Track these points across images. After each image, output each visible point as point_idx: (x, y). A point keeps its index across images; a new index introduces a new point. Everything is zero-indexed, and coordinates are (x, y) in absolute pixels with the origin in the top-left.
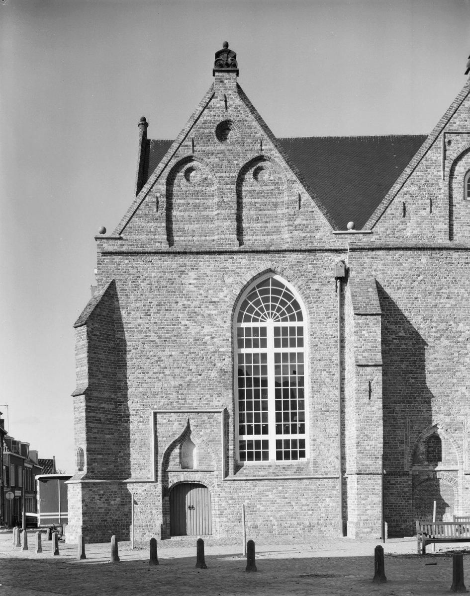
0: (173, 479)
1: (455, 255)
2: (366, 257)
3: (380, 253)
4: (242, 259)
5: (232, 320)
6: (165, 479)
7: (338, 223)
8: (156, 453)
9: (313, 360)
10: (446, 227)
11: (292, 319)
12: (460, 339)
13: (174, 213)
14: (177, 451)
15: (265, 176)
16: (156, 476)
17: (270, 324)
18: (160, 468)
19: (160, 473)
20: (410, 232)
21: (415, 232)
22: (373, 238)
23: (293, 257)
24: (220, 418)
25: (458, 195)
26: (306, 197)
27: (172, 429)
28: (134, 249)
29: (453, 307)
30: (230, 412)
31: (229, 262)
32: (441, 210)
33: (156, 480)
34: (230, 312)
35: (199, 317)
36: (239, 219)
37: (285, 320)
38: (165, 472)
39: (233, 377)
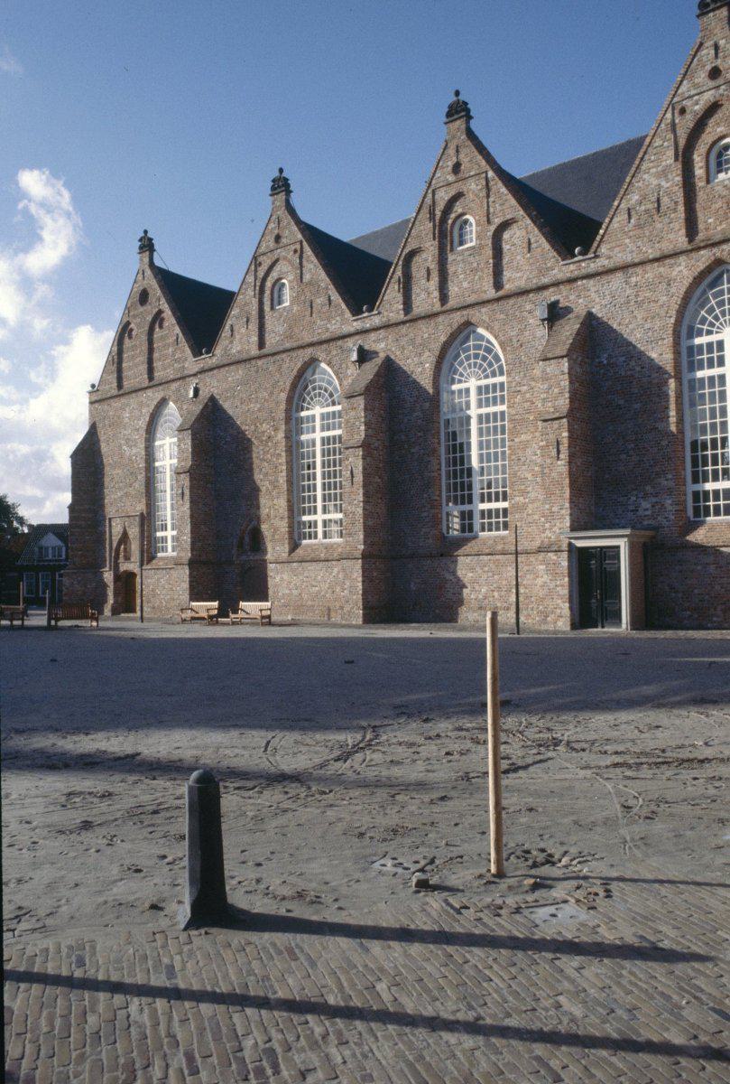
1: (260, 363)
2: (207, 377)
3: (215, 371)
4: (149, 393)
7: (197, 352)
10: (256, 339)
13: (124, 365)
15: (166, 324)
20: (236, 348)
21: (238, 349)
22: (214, 360)
23: (174, 386)
25: (267, 308)
26: (181, 335)
27: (117, 530)
28: (104, 397)
29: (259, 410)
31: (143, 396)
32: (254, 326)
36: (150, 361)
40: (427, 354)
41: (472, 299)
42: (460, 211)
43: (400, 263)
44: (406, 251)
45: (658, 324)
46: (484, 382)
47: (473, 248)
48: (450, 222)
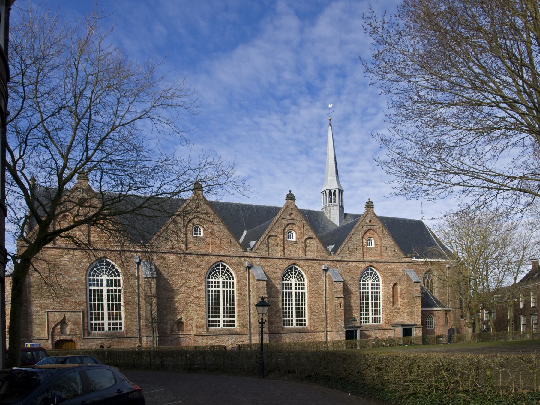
0: (57, 338)
5: (86, 275)
6: (53, 339)
8: (48, 328)
9: (125, 293)
11: (230, 279)
12: (191, 287)
14: (59, 327)
16: (48, 337)
17: (105, 278)
18: (51, 334)
19: (50, 336)
24: (81, 314)
30: (85, 312)
33: (48, 339)
34: (85, 272)
35: (70, 274)
37: (227, 279)
38: (53, 336)
39: (87, 298)
40: (278, 270)
41: (296, 257)
42: (290, 228)
43: (267, 238)
44: (269, 235)
45: (355, 277)
46: (297, 282)
47: (296, 241)
48: (286, 230)
